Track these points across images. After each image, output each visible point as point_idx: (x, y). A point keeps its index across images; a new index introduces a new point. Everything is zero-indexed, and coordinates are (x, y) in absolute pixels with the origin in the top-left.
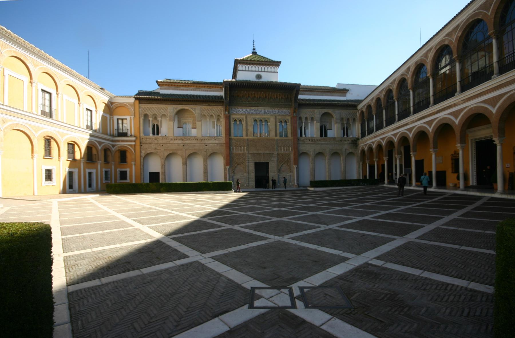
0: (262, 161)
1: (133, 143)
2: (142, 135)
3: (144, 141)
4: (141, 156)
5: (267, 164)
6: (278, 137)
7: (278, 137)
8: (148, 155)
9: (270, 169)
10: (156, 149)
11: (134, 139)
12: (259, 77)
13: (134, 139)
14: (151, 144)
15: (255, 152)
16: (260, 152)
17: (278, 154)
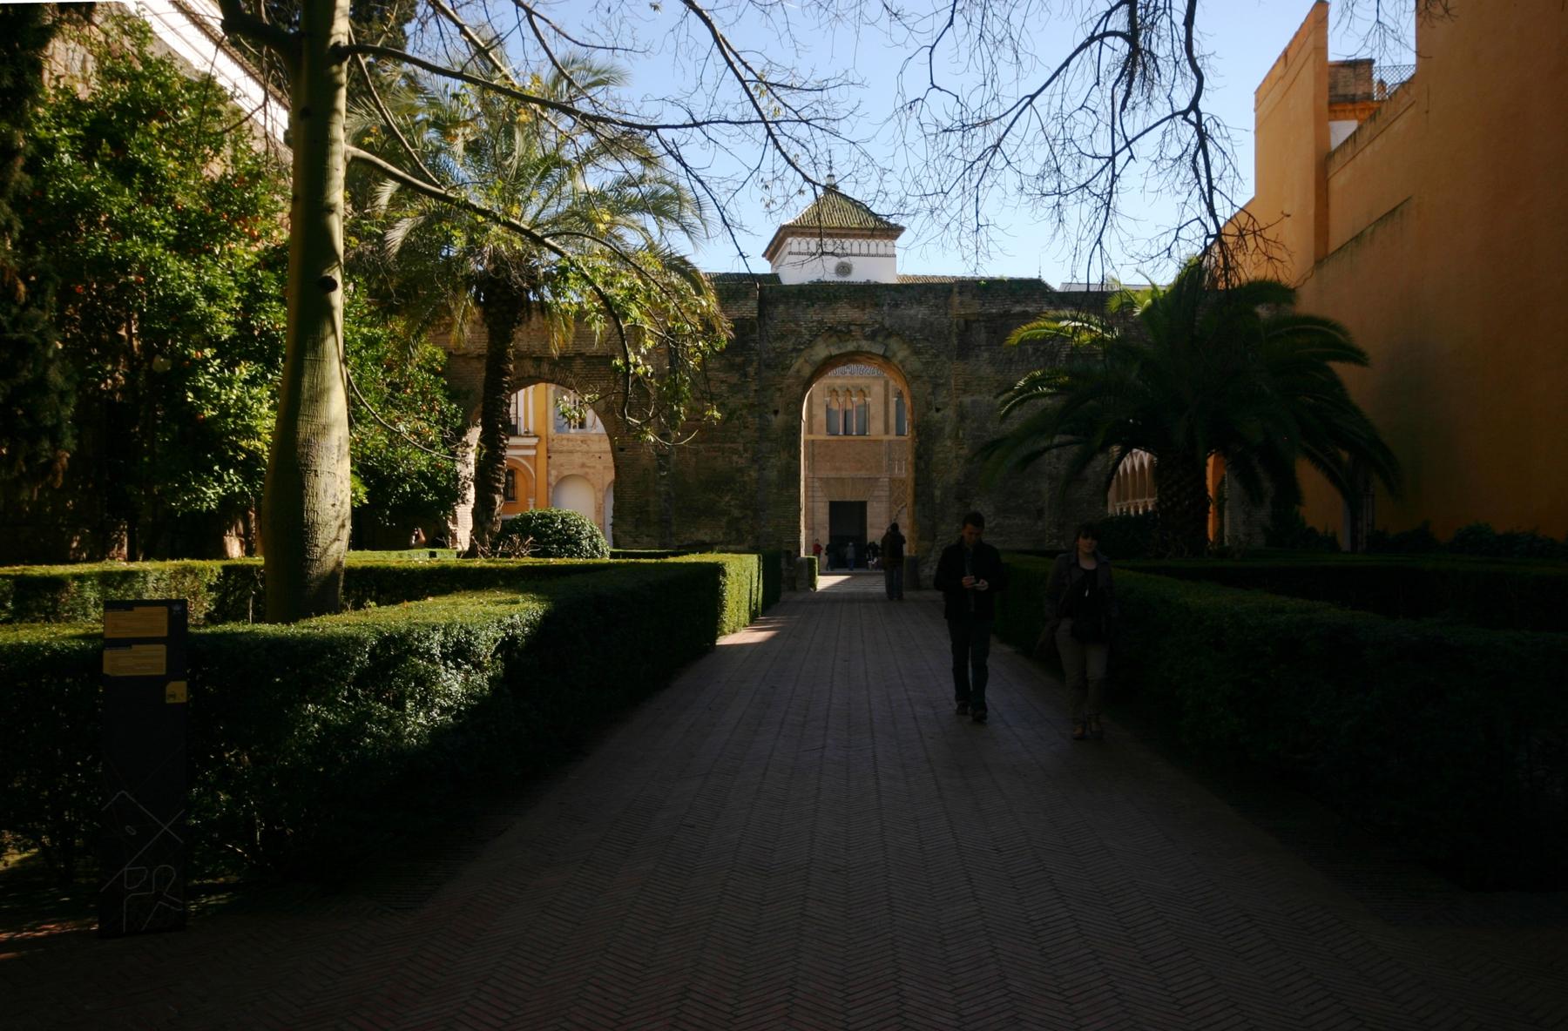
0: (850, 496)
1: (532, 452)
2: (551, 430)
3: (556, 445)
4: (549, 484)
5: (862, 506)
6: (892, 436)
7: (892, 436)
8: (562, 480)
9: (869, 520)
10: (583, 465)
11: (534, 441)
12: (844, 269)
13: (534, 441)
14: (571, 452)
15: (832, 474)
16: (844, 474)
17: (892, 480)
